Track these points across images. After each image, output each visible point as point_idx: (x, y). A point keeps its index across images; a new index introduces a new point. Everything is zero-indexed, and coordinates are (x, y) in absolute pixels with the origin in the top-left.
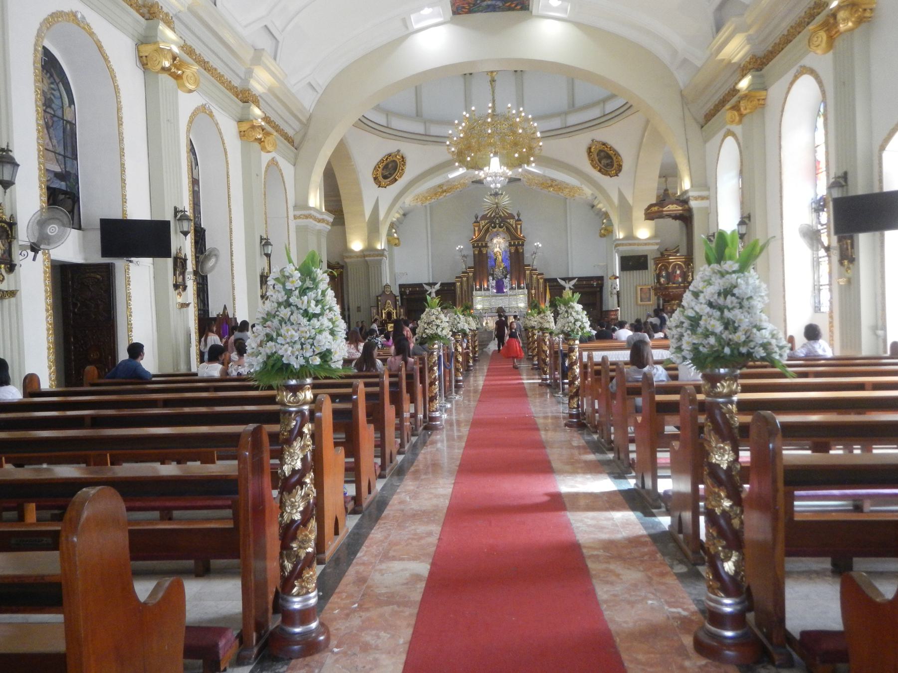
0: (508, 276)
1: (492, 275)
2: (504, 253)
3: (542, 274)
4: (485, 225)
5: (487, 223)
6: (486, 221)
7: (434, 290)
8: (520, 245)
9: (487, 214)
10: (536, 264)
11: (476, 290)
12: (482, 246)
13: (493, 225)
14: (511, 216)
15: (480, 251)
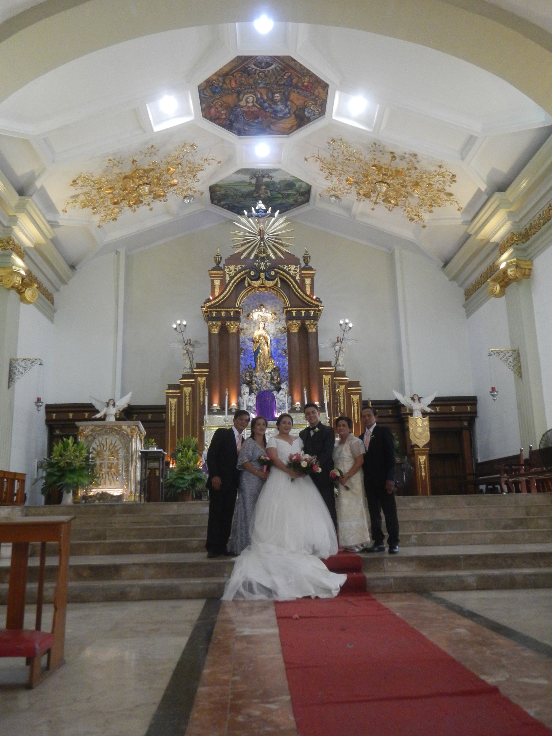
0: (284, 386)
1: (249, 384)
2: (274, 344)
3: (356, 384)
4: (236, 274)
5: (240, 271)
6: (239, 267)
7: (113, 411)
8: (310, 318)
9: (241, 253)
10: (342, 365)
11: (211, 412)
12: (229, 318)
13: (252, 273)
14: (291, 259)
15: (224, 330)
